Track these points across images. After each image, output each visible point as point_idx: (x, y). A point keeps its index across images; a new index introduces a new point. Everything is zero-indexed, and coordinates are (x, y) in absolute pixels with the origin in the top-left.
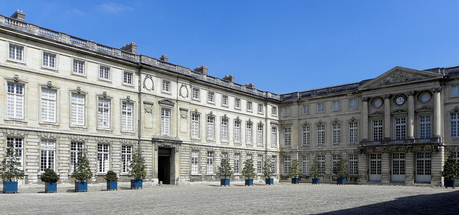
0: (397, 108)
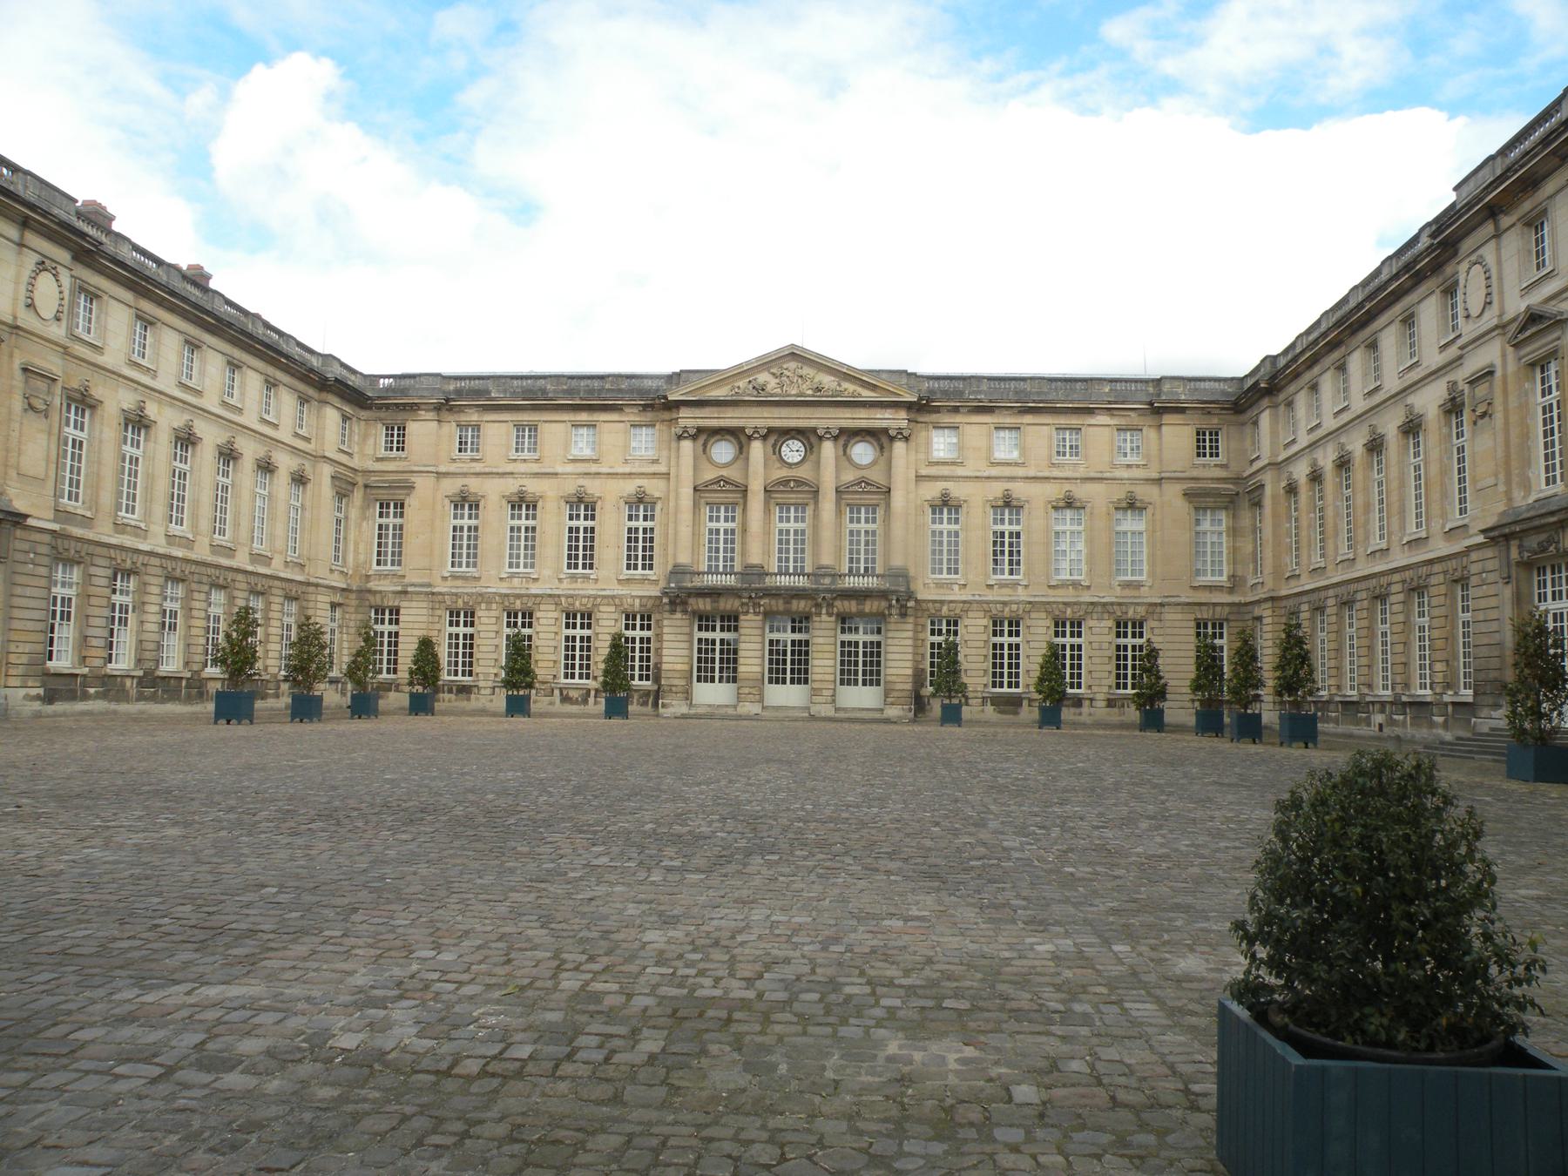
0: (784, 473)
